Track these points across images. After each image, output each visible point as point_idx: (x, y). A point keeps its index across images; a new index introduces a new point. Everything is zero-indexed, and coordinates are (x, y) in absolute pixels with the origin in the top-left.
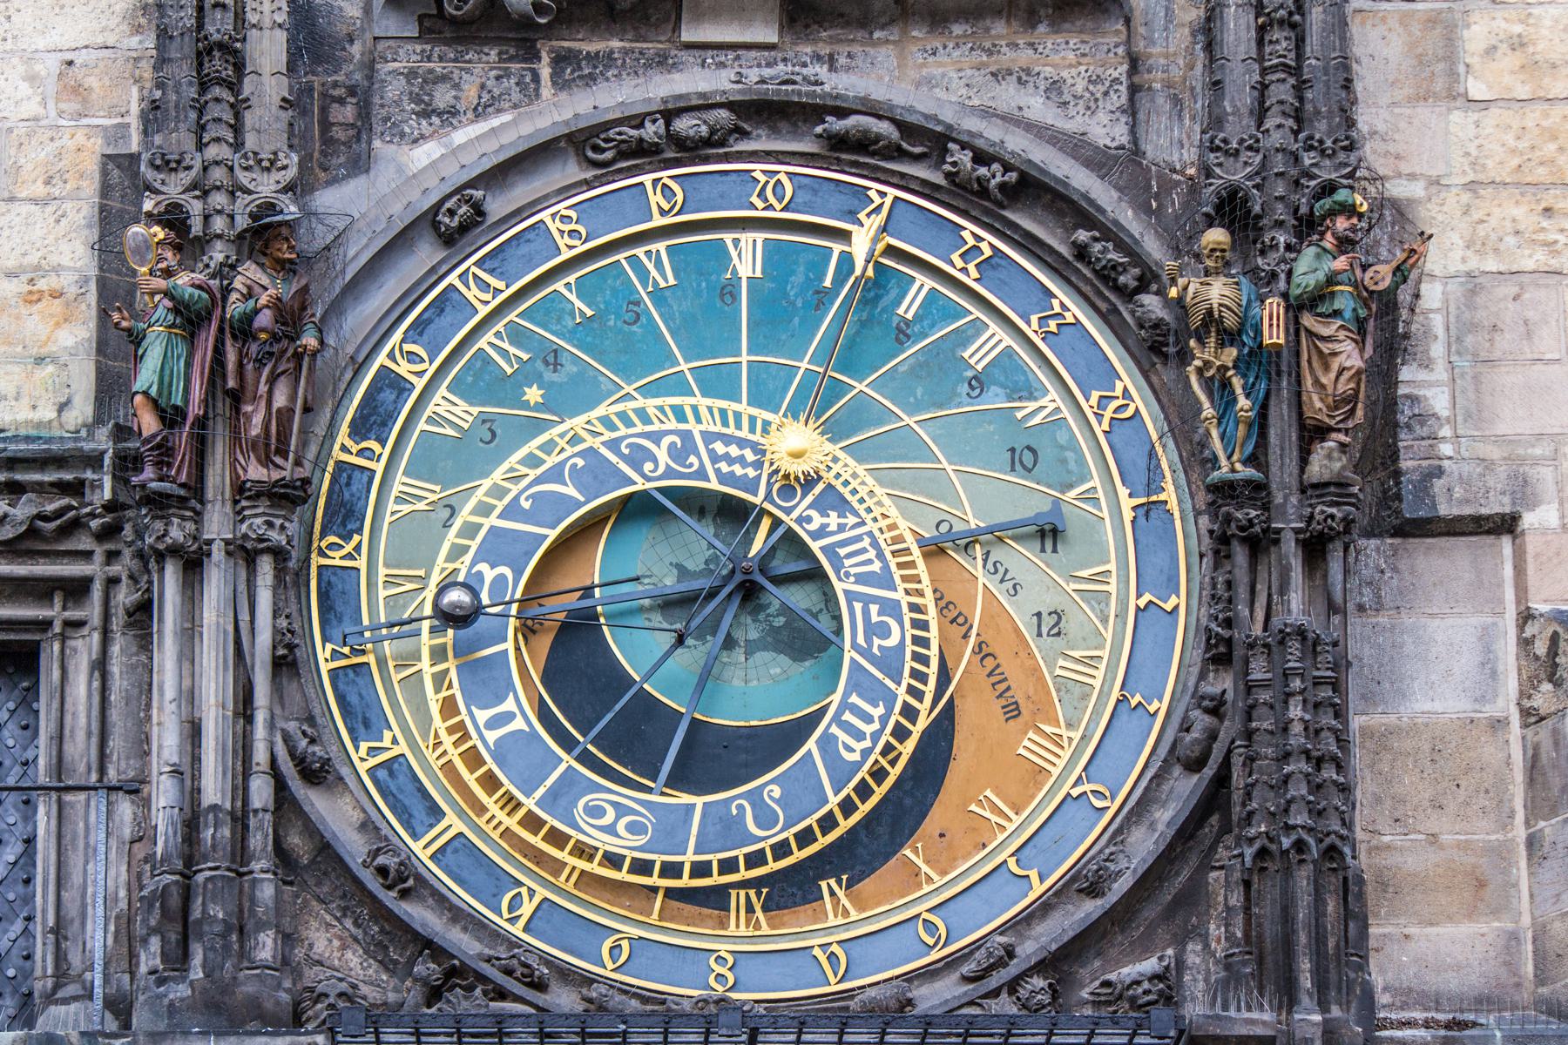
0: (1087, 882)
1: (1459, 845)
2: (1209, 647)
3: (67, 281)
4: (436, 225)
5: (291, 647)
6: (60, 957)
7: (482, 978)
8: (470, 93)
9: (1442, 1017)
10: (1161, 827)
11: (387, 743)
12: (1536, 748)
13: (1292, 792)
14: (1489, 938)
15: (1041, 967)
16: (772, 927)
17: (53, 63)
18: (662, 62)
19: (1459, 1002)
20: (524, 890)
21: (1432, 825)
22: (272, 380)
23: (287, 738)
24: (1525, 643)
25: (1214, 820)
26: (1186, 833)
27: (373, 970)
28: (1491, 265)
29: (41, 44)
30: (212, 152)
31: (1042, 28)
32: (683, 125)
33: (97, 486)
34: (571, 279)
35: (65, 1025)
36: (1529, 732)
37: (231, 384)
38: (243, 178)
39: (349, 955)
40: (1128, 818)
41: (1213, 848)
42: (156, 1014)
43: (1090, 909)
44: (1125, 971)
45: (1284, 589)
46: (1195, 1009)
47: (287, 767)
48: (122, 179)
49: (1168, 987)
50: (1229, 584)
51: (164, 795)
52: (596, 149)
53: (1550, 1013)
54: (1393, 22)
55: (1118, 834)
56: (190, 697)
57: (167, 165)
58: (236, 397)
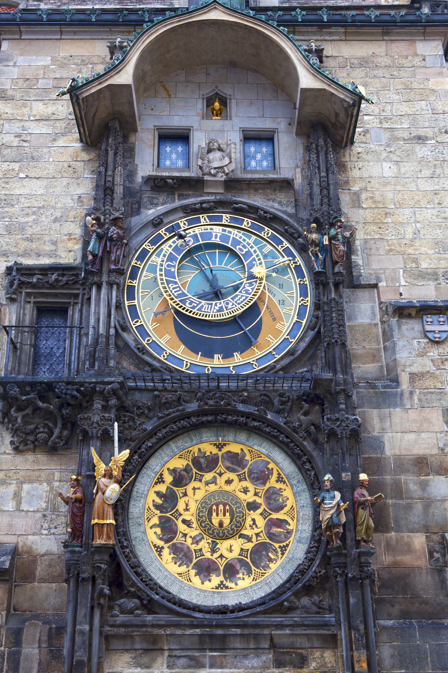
0: (291, 353)
1: (369, 348)
2: (315, 306)
3: (77, 236)
4: (153, 223)
5: (120, 304)
7: (160, 371)
8: (161, 200)
17: (76, 197)
18: (201, 196)
23: (118, 321)
24: (381, 308)
25: (318, 340)
28: (369, 237)
29: (74, 193)
30: (106, 207)
31: (277, 192)
32: (204, 205)
33: (81, 274)
41: (318, 346)
43: (292, 358)
45: (330, 293)
47: (118, 327)
50: (319, 293)
52: (186, 210)
54: (347, 194)
58: (109, 253)
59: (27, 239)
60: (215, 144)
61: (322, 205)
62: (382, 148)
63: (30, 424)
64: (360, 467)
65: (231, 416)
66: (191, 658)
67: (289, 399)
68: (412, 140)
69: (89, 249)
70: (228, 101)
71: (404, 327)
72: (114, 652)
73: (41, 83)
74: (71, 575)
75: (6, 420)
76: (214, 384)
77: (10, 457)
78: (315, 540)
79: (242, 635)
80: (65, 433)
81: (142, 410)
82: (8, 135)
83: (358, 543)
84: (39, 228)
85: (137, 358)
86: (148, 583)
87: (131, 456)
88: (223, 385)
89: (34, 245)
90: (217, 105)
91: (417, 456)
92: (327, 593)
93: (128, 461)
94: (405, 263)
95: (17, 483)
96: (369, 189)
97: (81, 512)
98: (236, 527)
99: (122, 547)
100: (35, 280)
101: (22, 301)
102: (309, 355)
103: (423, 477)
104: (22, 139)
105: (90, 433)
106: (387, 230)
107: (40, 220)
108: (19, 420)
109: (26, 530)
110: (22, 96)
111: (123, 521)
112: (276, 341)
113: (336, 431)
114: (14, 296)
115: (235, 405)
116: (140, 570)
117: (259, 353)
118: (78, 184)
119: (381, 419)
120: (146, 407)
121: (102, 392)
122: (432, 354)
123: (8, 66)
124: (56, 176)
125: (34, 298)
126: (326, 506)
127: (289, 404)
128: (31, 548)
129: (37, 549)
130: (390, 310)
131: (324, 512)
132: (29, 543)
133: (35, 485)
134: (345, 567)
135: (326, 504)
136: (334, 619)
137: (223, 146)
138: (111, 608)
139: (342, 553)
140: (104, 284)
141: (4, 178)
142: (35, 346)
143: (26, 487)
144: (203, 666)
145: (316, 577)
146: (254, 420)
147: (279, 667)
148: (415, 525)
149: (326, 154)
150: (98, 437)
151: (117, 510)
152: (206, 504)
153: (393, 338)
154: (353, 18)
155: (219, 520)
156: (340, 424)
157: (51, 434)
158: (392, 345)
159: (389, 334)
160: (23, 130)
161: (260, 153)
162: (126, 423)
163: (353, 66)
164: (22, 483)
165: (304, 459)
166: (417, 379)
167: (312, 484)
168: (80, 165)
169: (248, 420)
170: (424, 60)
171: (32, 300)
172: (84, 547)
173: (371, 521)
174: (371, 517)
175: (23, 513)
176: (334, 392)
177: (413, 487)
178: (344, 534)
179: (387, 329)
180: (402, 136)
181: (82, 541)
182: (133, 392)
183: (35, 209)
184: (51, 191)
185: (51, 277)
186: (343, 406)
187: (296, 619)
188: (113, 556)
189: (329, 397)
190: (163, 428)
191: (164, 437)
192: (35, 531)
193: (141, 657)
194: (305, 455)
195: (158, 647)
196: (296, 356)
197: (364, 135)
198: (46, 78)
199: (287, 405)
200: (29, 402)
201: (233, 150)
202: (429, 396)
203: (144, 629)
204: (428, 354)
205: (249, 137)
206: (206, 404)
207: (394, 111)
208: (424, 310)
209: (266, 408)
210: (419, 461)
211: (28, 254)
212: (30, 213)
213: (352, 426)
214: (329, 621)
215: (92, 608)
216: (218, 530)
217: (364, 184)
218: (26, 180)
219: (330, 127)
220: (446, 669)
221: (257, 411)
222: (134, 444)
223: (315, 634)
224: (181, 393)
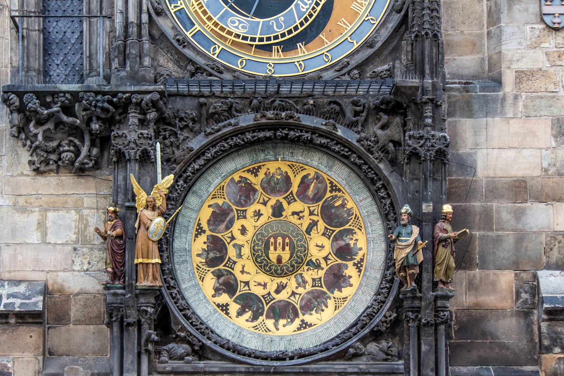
0: (369, 44)
1: (469, 34)
9: (463, 81)
10: (389, 29)
11: (179, 4)
12: (490, 7)
13: (425, 19)
14: (477, 60)
15: (357, 67)
16: (284, 56)
19: (468, 77)
20: (217, 46)
21: (462, 28)
23: (151, 3)
25: (404, 27)
26: (396, 30)
27: (176, 68)
35: (92, 83)
36: (489, 3)
39: (169, 64)
40: (380, 26)
41: (403, 35)
42: (117, 80)
43: (370, 51)
44: (379, 68)
46: (398, 79)
47: (152, 11)
49: (391, 73)
51: (119, 19)
53: (492, 80)
55: (377, 31)
63: (52, 141)
64: (445, 194)
65: (293, 130)
67: (364, 107)
74: (114, 319)
76: (272, 89)
77: (28, 179)
78: (387, 281)
80: (95, 151)
81: (186, 122)
83: (435, 285)
85: (176, 53)
86: (198, 327)
87: (176, 181)
88: (284, 89)
91: (515, 179)
92: (398, 338)
93: (172, 189)
95: (40, 211)
97: (121, 250)
98: (297, 263)
102: (390, 47)
103: (519, 205)
105: (127, 155)
108: (40, 137)
109: (55, 266)
111: (168, 258)
112: (351, 27)
115: (299, 118)
116: (189, 313)
117: (329, 44)
119: (475, 132)
120: (191, 119)
122: (547, 45)
127: (364, 114)
128: (62, 286)
129: (69, 288)
131: (398, 250)
132: (59, 280)
133: (61, 212)
134: (419, 312)
135: (401, 241)
138: (158, 353)
139: (416, 297)
142: (44, 31)
145: (386, 322)
146: (320, 136)
148: (504, 261)
151: (162, 245)
155: (277, 255)
156: (424, 144)
157: (77, 153)
158: (498, 31)
159: (495, 16)
162: (166, 139)
164: (46, 210)
165: (379, 184)
169: (314, 136)
172: (127, 289)
173: (452, 260)
174: (453, 255)
175: (50, 246)
176: (419, 101)
177: (506, 216)
179: (493, 8)
182: (174, 98)
188: (159, 297)
189: (413, 106)
190: (212, 147)
191: (214, 158)
194: (380, 179)
196: (376, 48)
199: (362, 116)
200: (51, 116)
202: (537, 102)
204: (542, 45)
206: (264, 116)
209: (336, 121)
210: (517, 184)
213: (437, 147)
214: (398, 369)
215: (139, 354)
216: (276, 266)
221: (326, 125)
222: (178, 167)
224: (233, 100)
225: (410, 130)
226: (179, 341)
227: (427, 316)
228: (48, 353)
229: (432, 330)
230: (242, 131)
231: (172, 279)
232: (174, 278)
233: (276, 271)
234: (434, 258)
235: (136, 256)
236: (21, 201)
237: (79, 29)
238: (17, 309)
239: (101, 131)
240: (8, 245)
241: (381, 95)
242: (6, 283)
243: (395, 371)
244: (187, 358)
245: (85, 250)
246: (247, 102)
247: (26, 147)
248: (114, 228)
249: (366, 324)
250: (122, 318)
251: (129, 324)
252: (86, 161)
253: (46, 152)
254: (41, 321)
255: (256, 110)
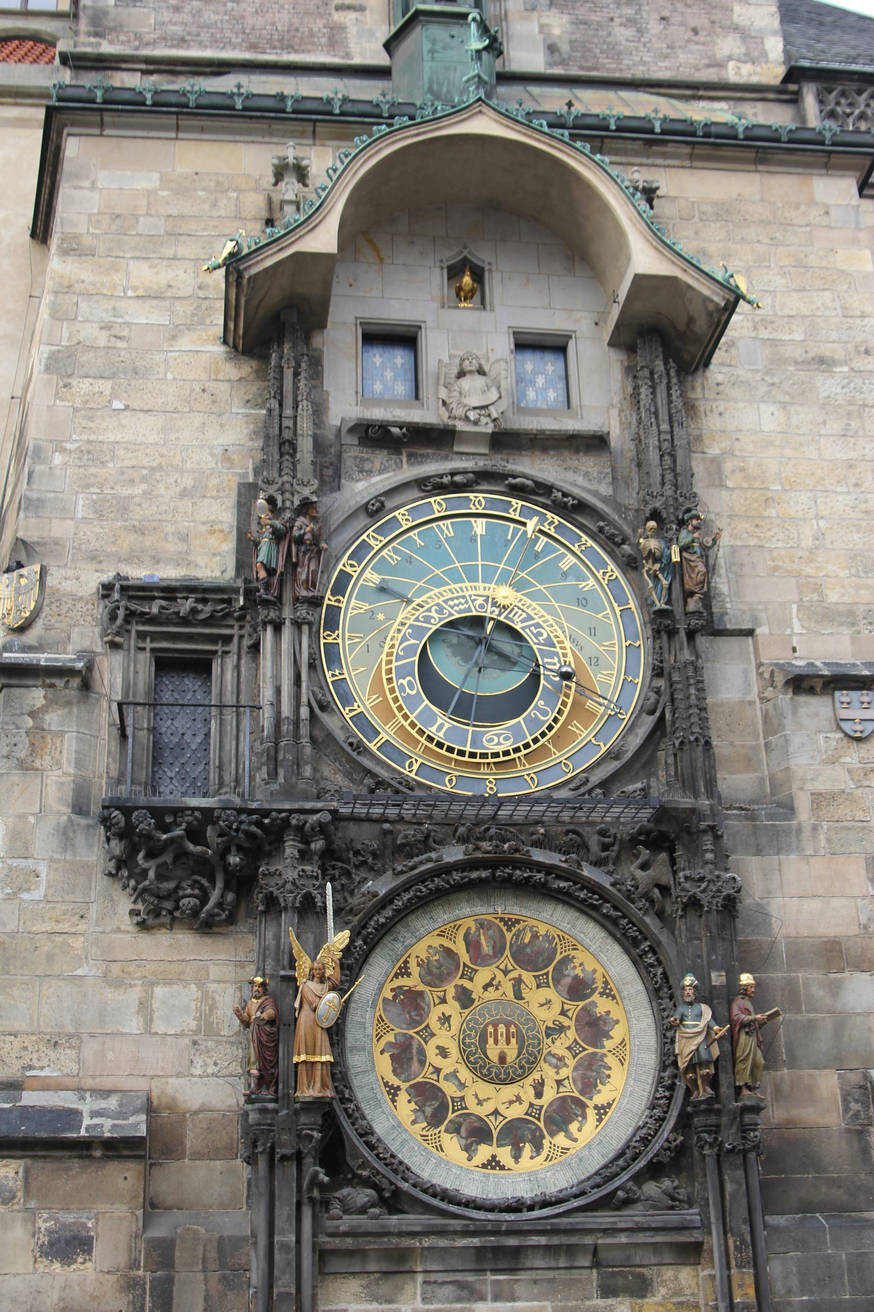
0: (612, 755)
2: (653, 669)
3: (225, 526)
4: (367, 509)
5: (314, 659)
6: (221, 777)
7: (390, 785)
8: (377, 464)
17: (219, 451)
18: (446, 458)
22: (310, 559)
23: (314, 693)
24: (760, 675)
28: (739, 543)
30: (285, 478)
31: (581, 454)
32: (458, 478)
33: (238, 600)
34: (416, 531)
36: (763, 706)
37: (294, 560)
38: (297, 488)
43: (615, 765)
48: (247, 493)
50: (661, 648)
52: (426, 486)
56: (277, 677)
57: (268, 482)
58: (295, 566)
59: (134, 529)
60: (474, 361)
61: (663, 484)
62: (758, 377)
66: (461, 1285)
68: (809, 363)
69: (260, 559)
70: (486, 274)
71: (803, 711)
72: (332, 1277)
73: (144, 225)
74: (260, 1149)
75: (125, 873)
79: (547, 1247)
82: (87, 325)
83: (738, 1090)
84: (154, 508)
85: (347, 762)
86: (388, 1161)
87: (352, 940)
89: (148, 541)
90: (468, 280)
92: (684, 1174)
93: (347, 951)
94: (800, 593)
95: (143, 985)
96: (737, 453)
98: (528, 1062)
99: (343, 1100)
100: (155, 610)
101: (132, 647)
102: (643, 761)
104: (114, 332)
105: (281, 900)
106: (769, 530)
107: (156, 492)
108: (151, 874)
110: (110, 249)
112: (586, 732)
113: (699, 900)
114: (118, 639)
115: (528, 851)
117: (558, 754)
118: (222, 425)
119: (765, 875)
121: (300, 829)
122: (848, 760)
123: (81, 188)
124: (180, 409)
125: (152, 641)
126: (688, 1031)
127: (616, 848)
129: (185, 1102)
130: (780, 679)
132: (170, 1091)
133: (175, 987)
134: (717, 1132)
136: (698, 1217)
137: (486, 368)
138: (326, 1204)
140: (288, 623)
141: (85, 409)
143: (160, 991)
144: (482, 1298)
145: (669, 1149)
146: (559, 877)
147: (607, 1297)
149: (669, 388)
150: (294, 908)
152: (476, 1022)
153: (783, 729)
154: (706, 129)
157: (204, 898)
160: (115, 316)
161: (542, 373)
163: (704, 217)
164: (152, 984)
165: (645, 946)
166: (824, 803)
167: (657, 990)
168: (222, 389)
169: (549, 878)
170: (827, 213)
171: (148, 644)
173: (759, 1054)
175: (157, 1038)
176: (694, 830)
177: (818, 992)
178: (716, 1077)
179: (772, 712)
180: (791, 355)
181: (276, 1091)
182: (345, 823)
183: (145, 472)
184: (173, 437)
185: (183, 605)
186: (709, 856)
187: (636, 1219)
191: (406, 907)
192: (180, 1069)
193: (378, 1284)
194: (646, 939)
195: (407, 1268)
197: (726, 351)
198: (152, 216)
201: (503, 374)
203: (386, 1239)
204: (842, 760)
205: (526, 344)
206: (477, 848)
207: (778, 308)
208: (840, 682)
211: (138, 558)
212: (137, 480)
214: (691, 1221)
215: (299, 1205)
216: (497, 1068)
217: (729, 443)
218: (126, 413)
219: (672, 337)
220: (873, 1292)
221: (566, 861)
223: (667, 1243)
224: (431, 827)
225: (684, 869)
226: (357, 1184)
227: (729, 1139)
228: (152, 1206)
229: (739, 1160)
230: (448, 869)
231: (345, 1086)
232: (348, 1087)
233: (497, 1075)
234: (733, 1052)
235: (296, 1051)
236: (115, 969)
237: (204, 731)
238: (107, 1135)
239: (241, 868)
240: (92, 1036)
241: (636, 823)
242: (88, 1094)
243: (687, 1224)
244: (372, 1210)
245: (210, 1044)
246: (450, 830)
247: (128, 890)
248: (262, 1008)
249: (640, 1153)
250: (273, 1148)
251: (284, 1158)
252: (216, 910)
253: (158, 897)
254: (143, 1153)
255: (463, 840)
